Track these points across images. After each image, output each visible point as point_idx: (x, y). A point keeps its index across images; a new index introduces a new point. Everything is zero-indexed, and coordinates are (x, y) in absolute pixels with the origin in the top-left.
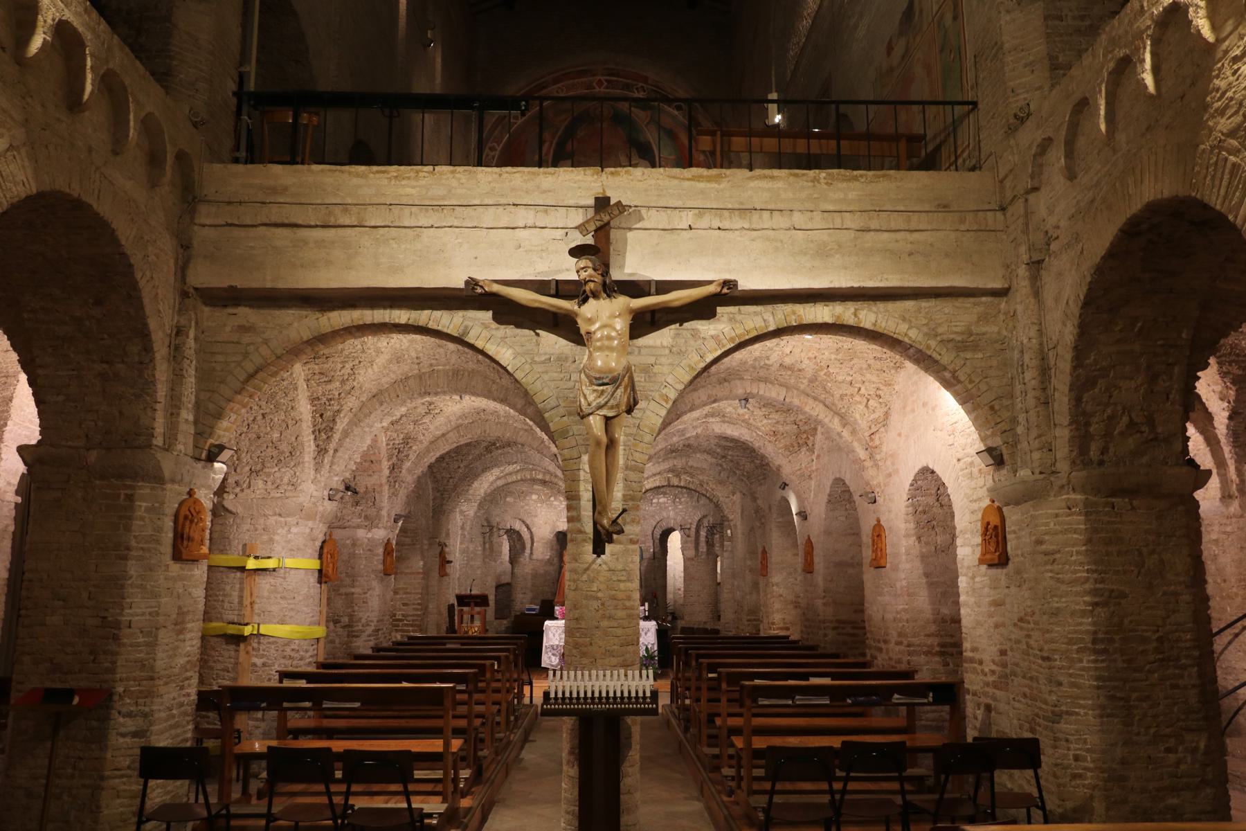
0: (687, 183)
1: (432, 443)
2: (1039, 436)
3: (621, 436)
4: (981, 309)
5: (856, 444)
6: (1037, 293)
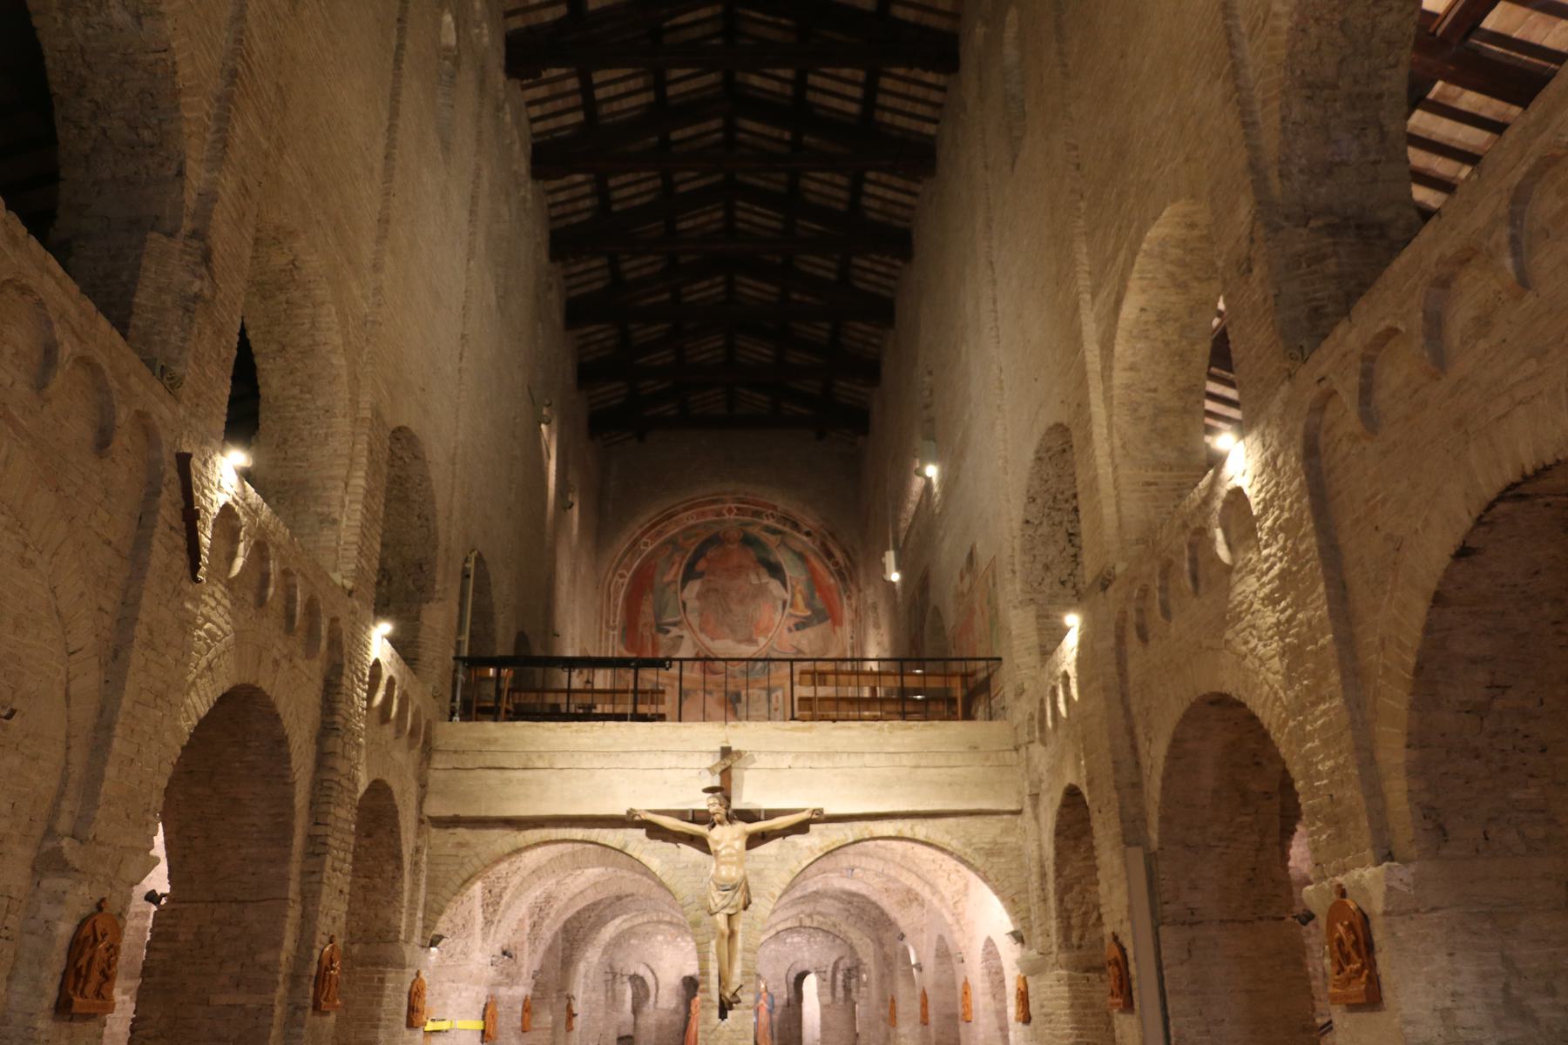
0: (788, 733)
1: (571, 899)
2: (1041, 925)
3: (739, 927)
4: (1003, 824)
5: (944, 911)
6: (1036, 818)
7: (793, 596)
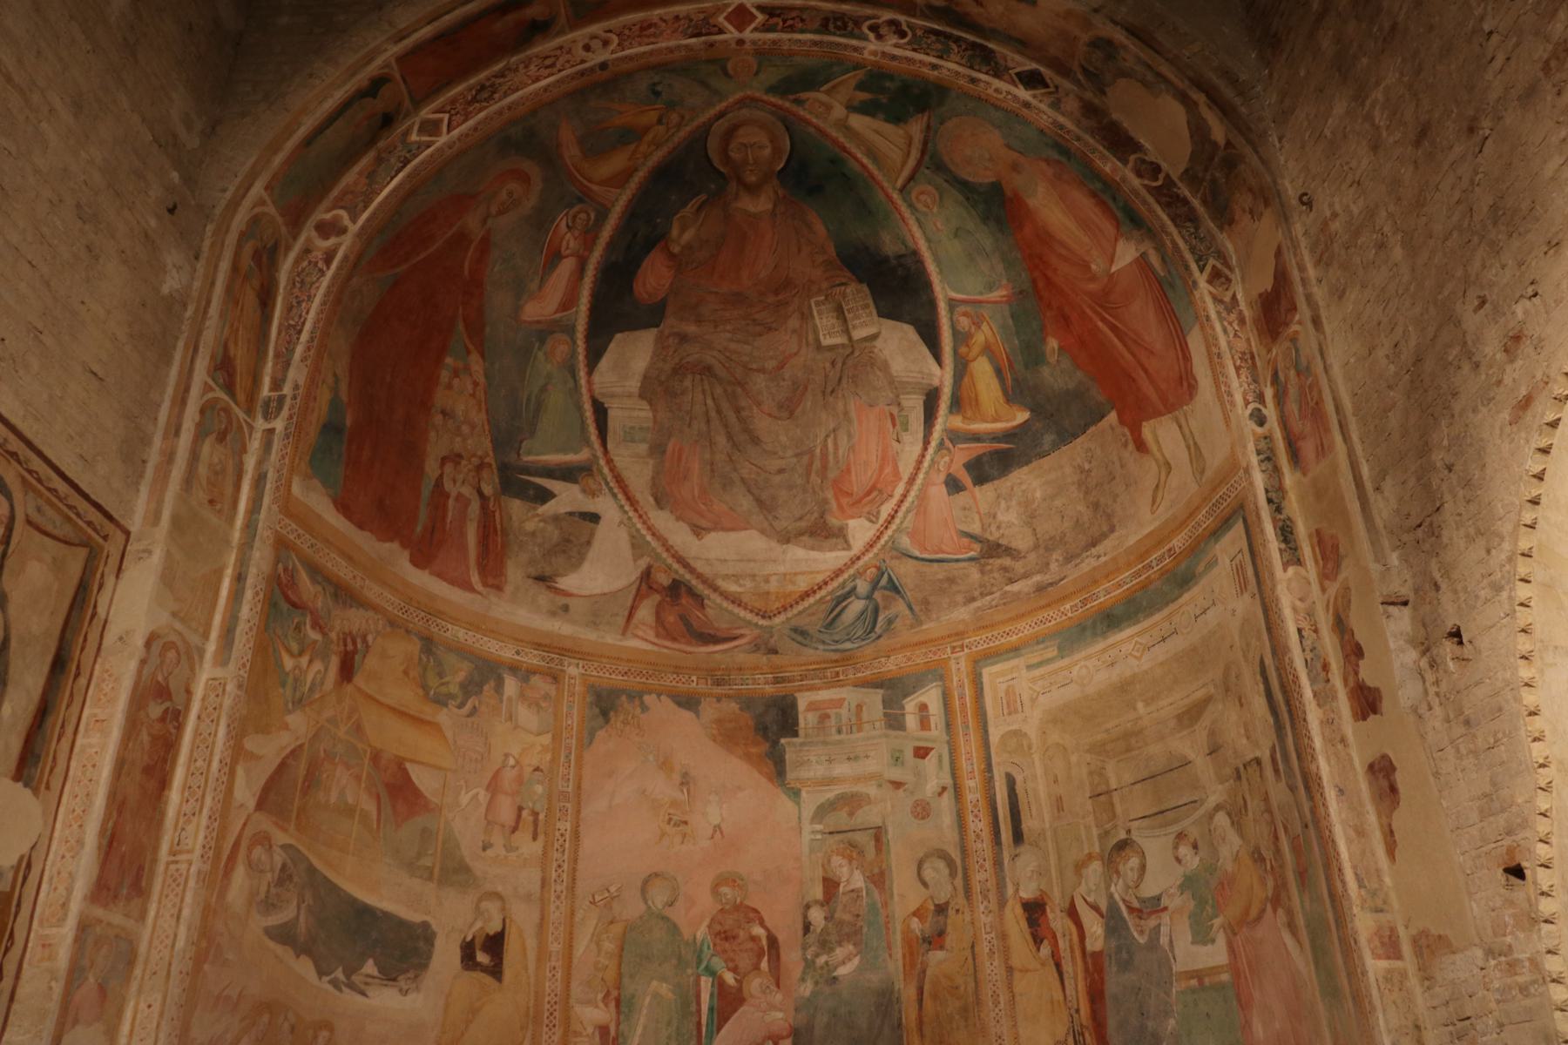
7: (962, 369)
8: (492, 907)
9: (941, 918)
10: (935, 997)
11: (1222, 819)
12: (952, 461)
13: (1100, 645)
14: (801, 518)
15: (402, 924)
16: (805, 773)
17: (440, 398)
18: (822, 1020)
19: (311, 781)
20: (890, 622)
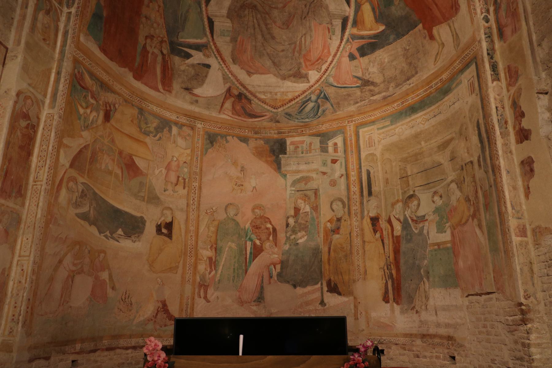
8: (168, 212)
9: (339, 223)
10: (335, 251)
11: (453, 186)
12: (352, 47)
13: (408, 119)
14: (290, 70)
15: (132, 217)
16: (288, 168)
17: (145, 11)
18: (292, 258)
19: (93, 159)
20: (324, 111)
